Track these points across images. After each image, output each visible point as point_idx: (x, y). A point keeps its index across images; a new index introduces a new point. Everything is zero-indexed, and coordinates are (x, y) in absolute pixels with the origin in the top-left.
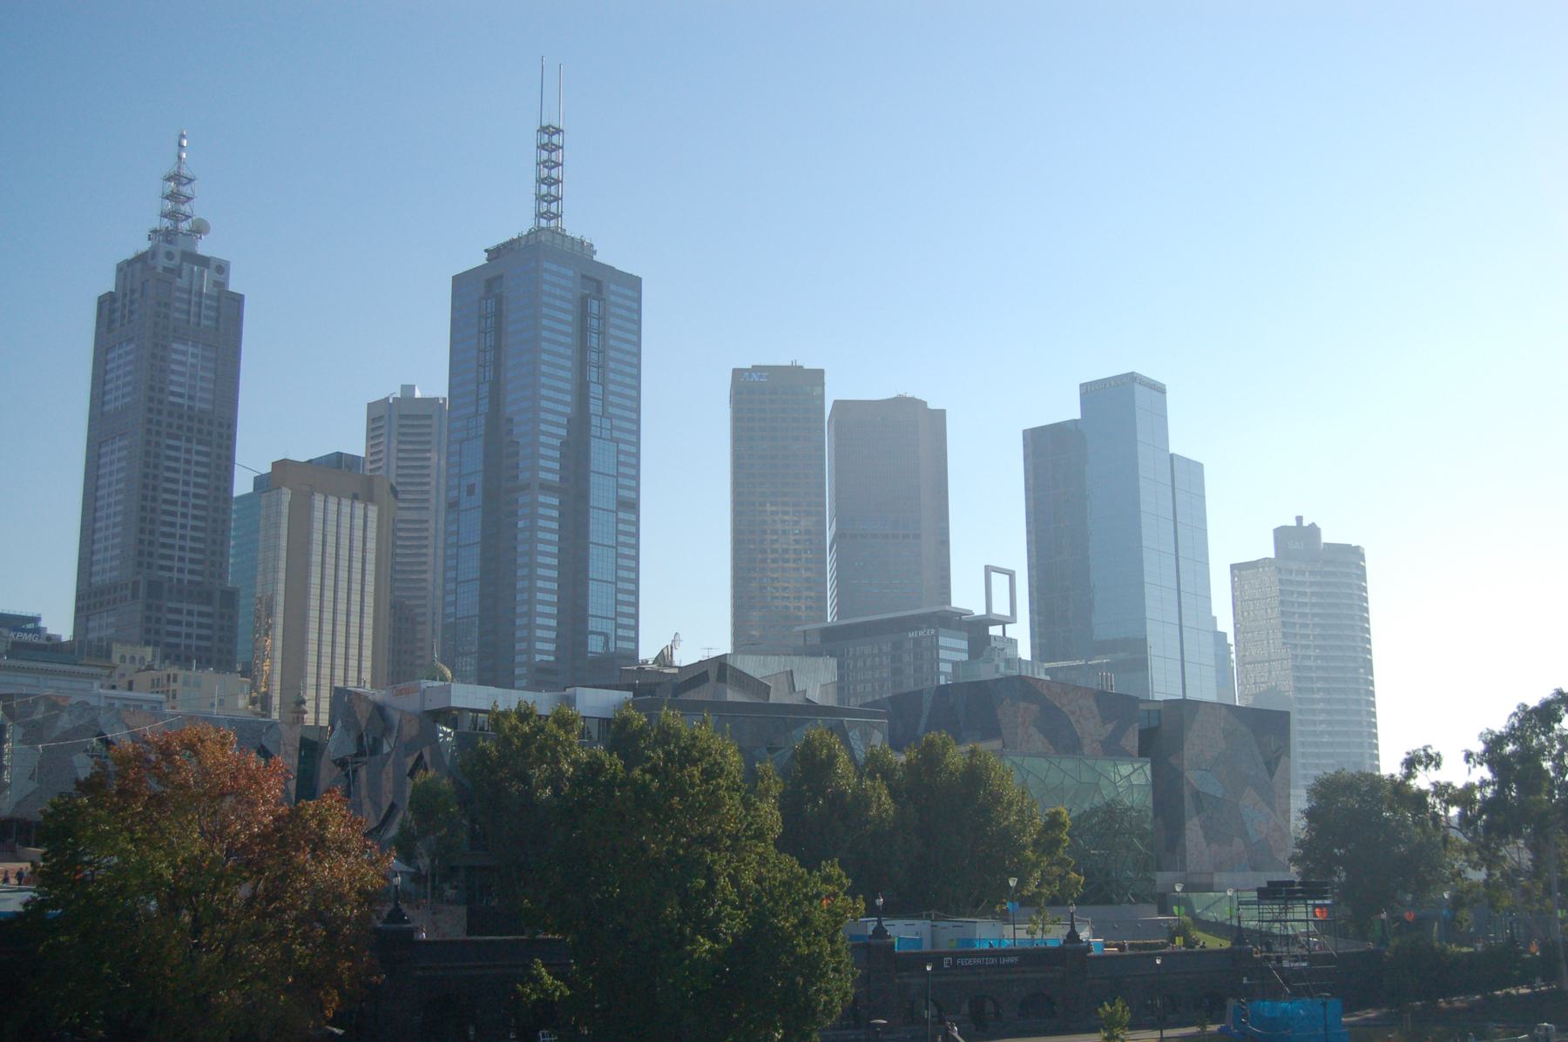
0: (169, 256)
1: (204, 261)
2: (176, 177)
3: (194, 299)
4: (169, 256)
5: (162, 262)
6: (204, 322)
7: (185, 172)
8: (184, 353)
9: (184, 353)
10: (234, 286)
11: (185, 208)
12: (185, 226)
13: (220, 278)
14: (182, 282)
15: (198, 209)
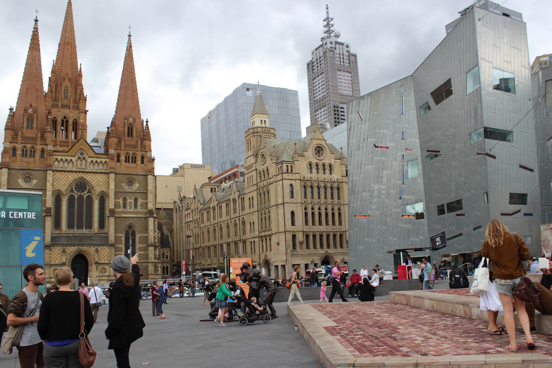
0: (331, 43)
1: (342, 44)
2: (327, 18)
3: (342, 57)
4: (331, 43)
5: (329, 45)
6: (346, 64)
7: (330, 17)
8: (341, 75)
9: (341, 75)
10: (352, 51)
11: (332, 29)
12: (333, 34)
13: (348, 49)
14: (337, 51)
15: (336, 28)
